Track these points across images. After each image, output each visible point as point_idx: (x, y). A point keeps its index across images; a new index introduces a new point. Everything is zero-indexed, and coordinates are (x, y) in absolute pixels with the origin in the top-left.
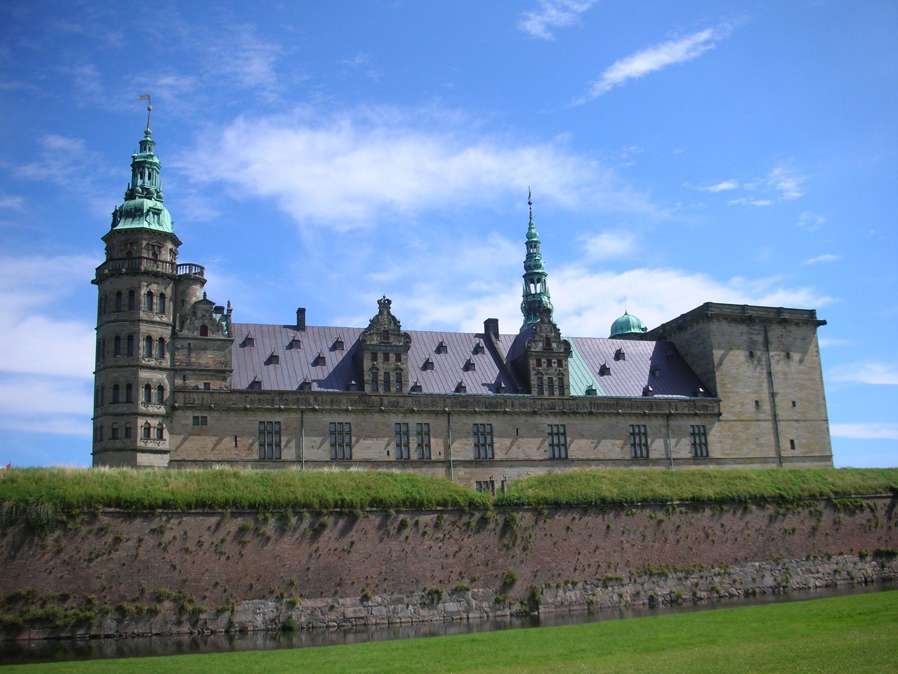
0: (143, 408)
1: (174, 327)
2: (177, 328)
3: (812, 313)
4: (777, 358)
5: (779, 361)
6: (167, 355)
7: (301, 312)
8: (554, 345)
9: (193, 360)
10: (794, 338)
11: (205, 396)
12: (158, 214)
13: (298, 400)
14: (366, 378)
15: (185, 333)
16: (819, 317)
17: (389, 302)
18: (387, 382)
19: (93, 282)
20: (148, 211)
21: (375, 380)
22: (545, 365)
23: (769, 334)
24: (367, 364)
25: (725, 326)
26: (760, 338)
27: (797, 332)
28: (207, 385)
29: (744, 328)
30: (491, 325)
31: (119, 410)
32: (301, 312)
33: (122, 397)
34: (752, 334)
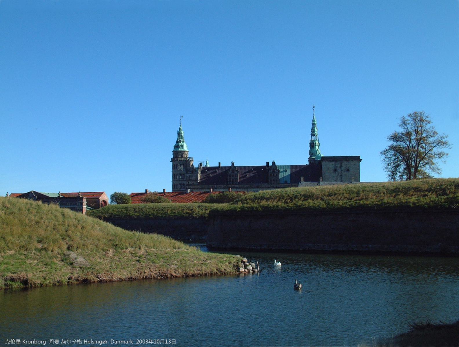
0: (180, 189)
1: (186, 171)
2: (187, 172)
3: (359, 157)
4: (344, 171)
5: (344, 172)
6: (185, 178)
7: (219, 163)
8: (275, 171)
9: (190, 179)
10: (351, 165)
11: (193, 186)
12: (182, 146)
13: (213, 186)
14: (228, 180)
15: (189, 172)
16: (361, 158)
17: (234, 163)
18: (233, 181)
19: (171, 162)
20: (180, 146)
21: (230, 181)
22: (272, 176)
23: (342, 164)
24: (228, 178)
25: (327, 162)
26: (339, 165)
27: (352, 163)
28: (193, 184)
29: (334, 163)
30: (268, 163)
31: (175, 190)
32: (219, 163)
33: (176, 187)
34: (336, 164)
